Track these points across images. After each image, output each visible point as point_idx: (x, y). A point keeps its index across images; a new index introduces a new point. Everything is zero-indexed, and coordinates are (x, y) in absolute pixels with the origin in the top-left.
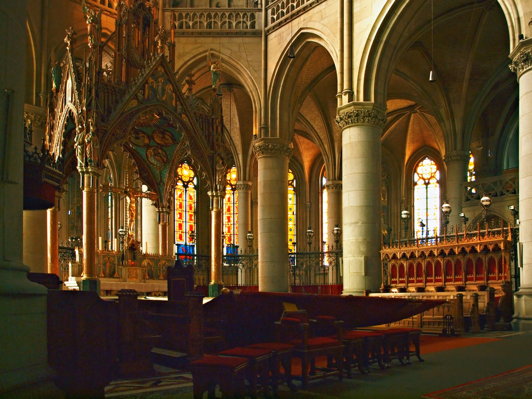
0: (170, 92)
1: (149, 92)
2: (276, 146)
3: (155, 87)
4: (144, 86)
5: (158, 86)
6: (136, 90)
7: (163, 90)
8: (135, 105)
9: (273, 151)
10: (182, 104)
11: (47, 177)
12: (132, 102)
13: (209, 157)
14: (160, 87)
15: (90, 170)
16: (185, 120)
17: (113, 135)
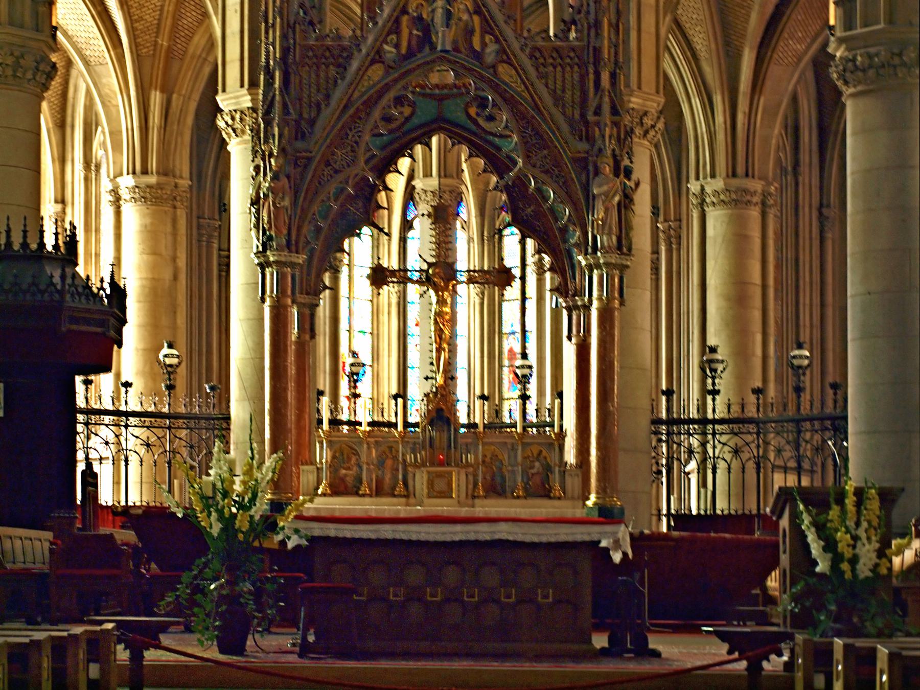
0: (465, 17)
1: (411, 33)
2: (877, 55)
3: (425, 16)
4: (397, 21)
5: (433, 11)
6: (376, 40)
7: (448, 15)
8: (376, 79)
9: (871, 73)
10: (497, 41)
11: (74, 320)
12: (370, 72)
13: (574, 160)
14: (440, 11)
15: (271, 259)
16: (507, 79)
17: (328, 164)
